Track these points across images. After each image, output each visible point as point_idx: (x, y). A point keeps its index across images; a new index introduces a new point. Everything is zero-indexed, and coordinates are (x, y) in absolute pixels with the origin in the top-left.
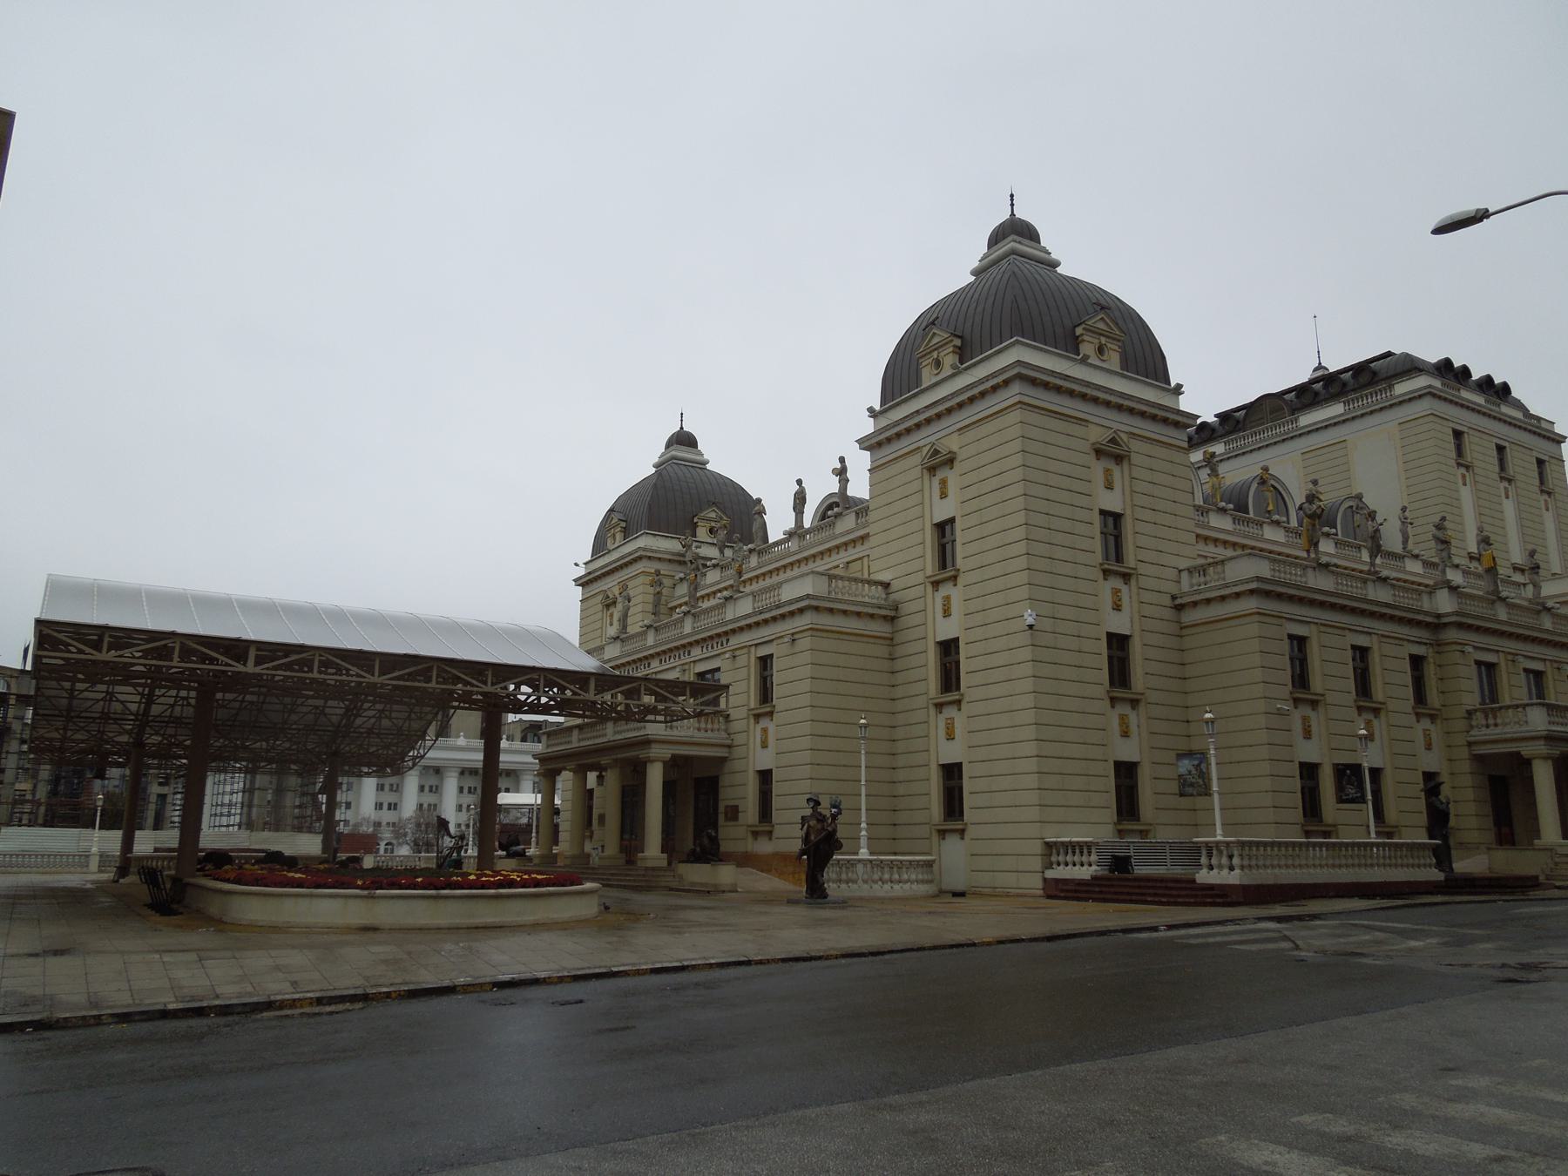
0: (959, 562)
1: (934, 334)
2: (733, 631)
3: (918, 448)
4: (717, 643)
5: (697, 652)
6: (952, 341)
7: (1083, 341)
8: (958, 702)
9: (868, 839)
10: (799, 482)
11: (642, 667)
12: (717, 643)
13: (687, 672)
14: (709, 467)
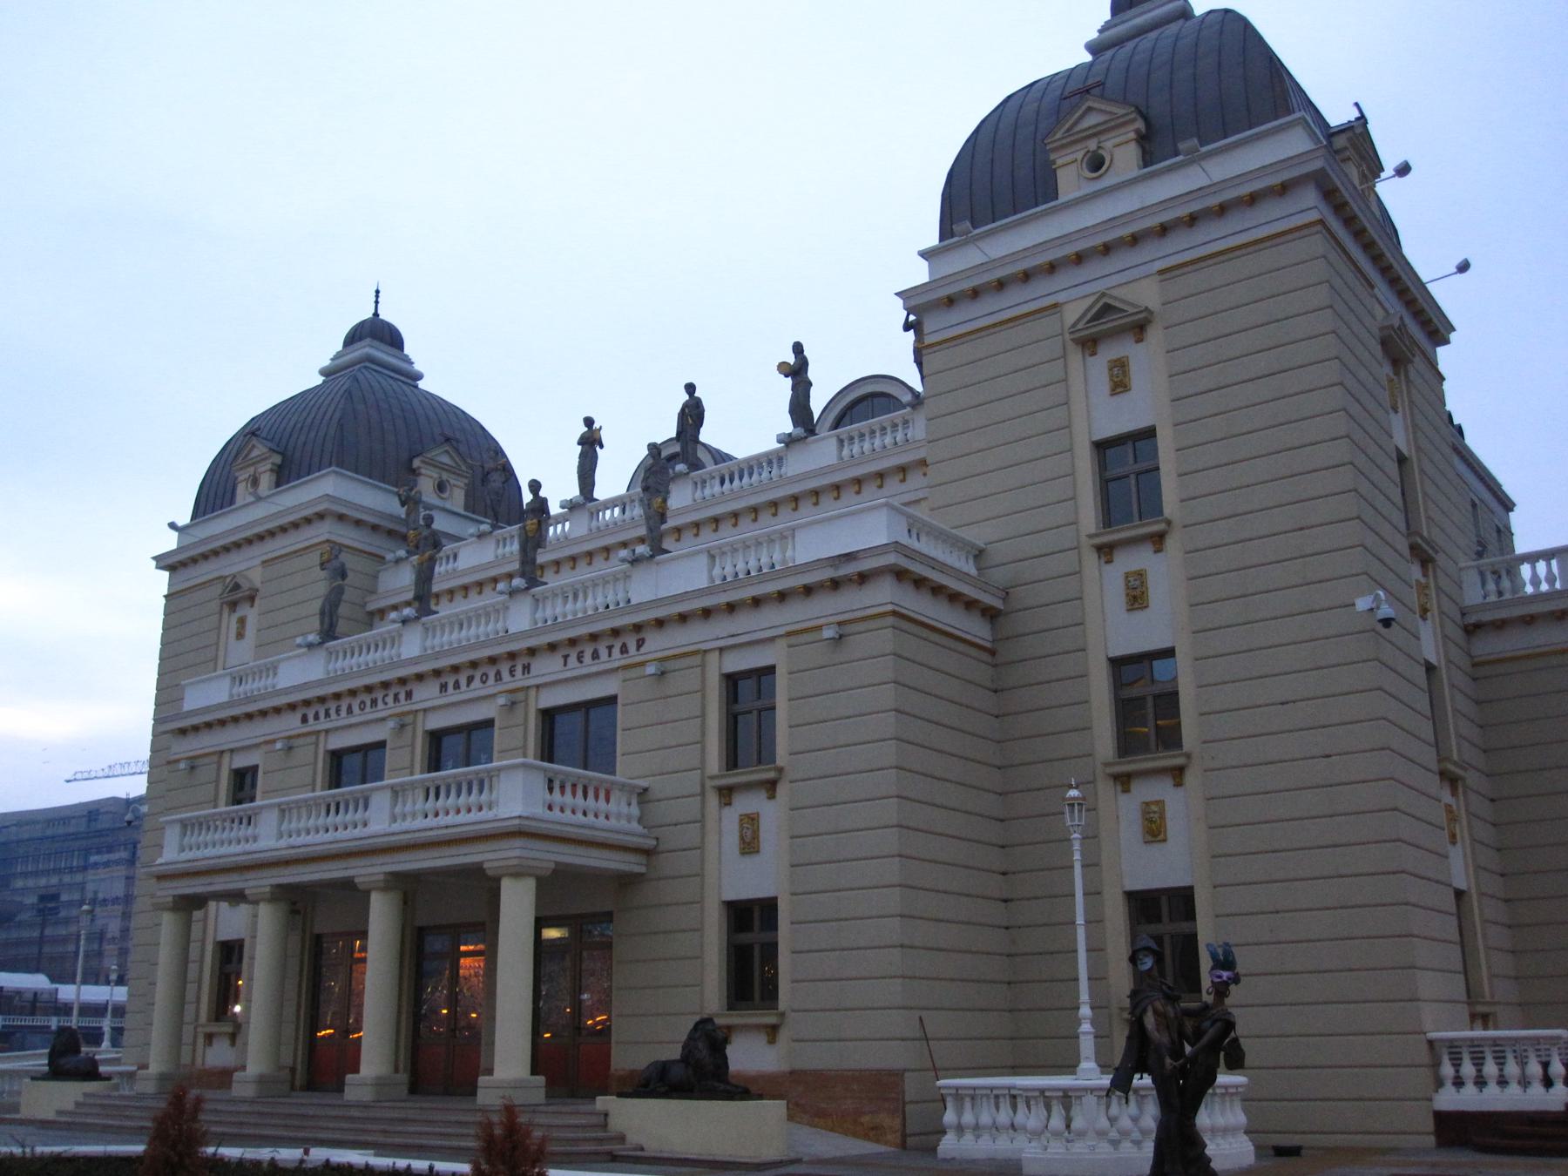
0: (1170, 503)
1: (1090, 109)
2: (660, 623)
3: (1055, 306)
4: (610, 648)
5: (546, 668)
6: (1133, 121)
8: (1178, 774)
9: (1096, 1037)
10: (690, 388)
11: (390, 699)
12: (610, 648)
13: (409, 728)
14: (422, 384)
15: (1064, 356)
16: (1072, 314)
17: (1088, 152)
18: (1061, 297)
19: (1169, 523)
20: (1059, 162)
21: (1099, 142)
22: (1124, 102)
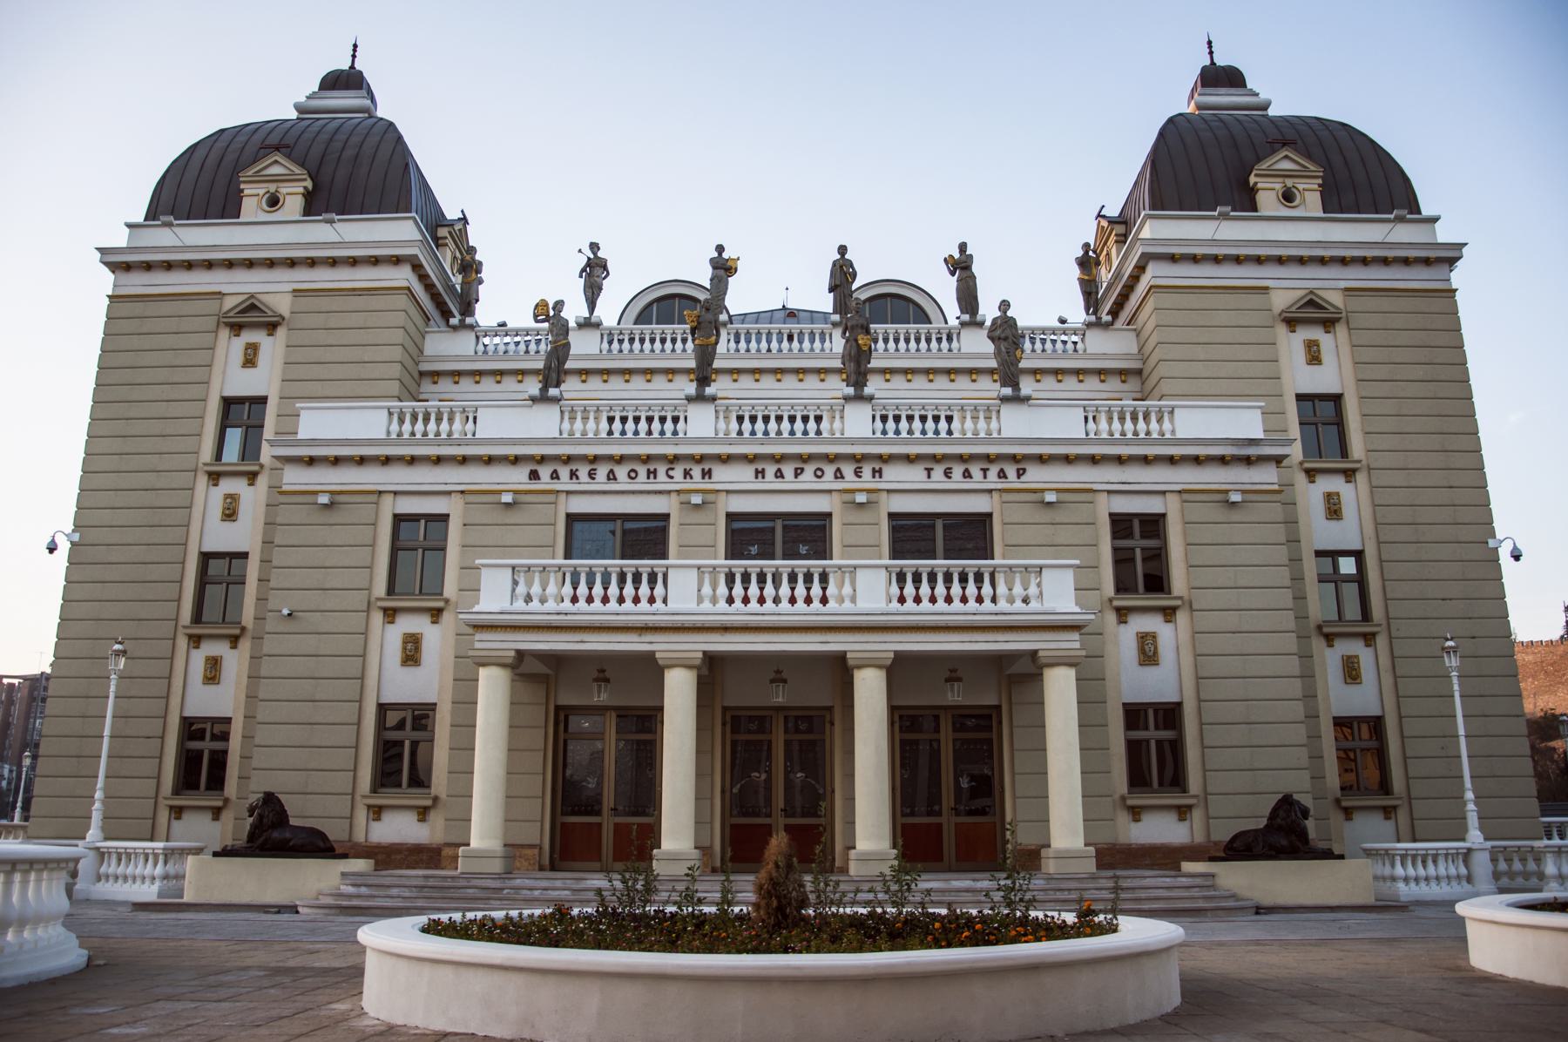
1: (276, 162)
6: (305, 180)
7: (447, 245)
15: (216, 332)
16: (229, 303)
17: (268, 192)
18: (225, 289)
19: (262, 466)
20: (246, 192)
21: (278, 187)
22: (302, 165)
